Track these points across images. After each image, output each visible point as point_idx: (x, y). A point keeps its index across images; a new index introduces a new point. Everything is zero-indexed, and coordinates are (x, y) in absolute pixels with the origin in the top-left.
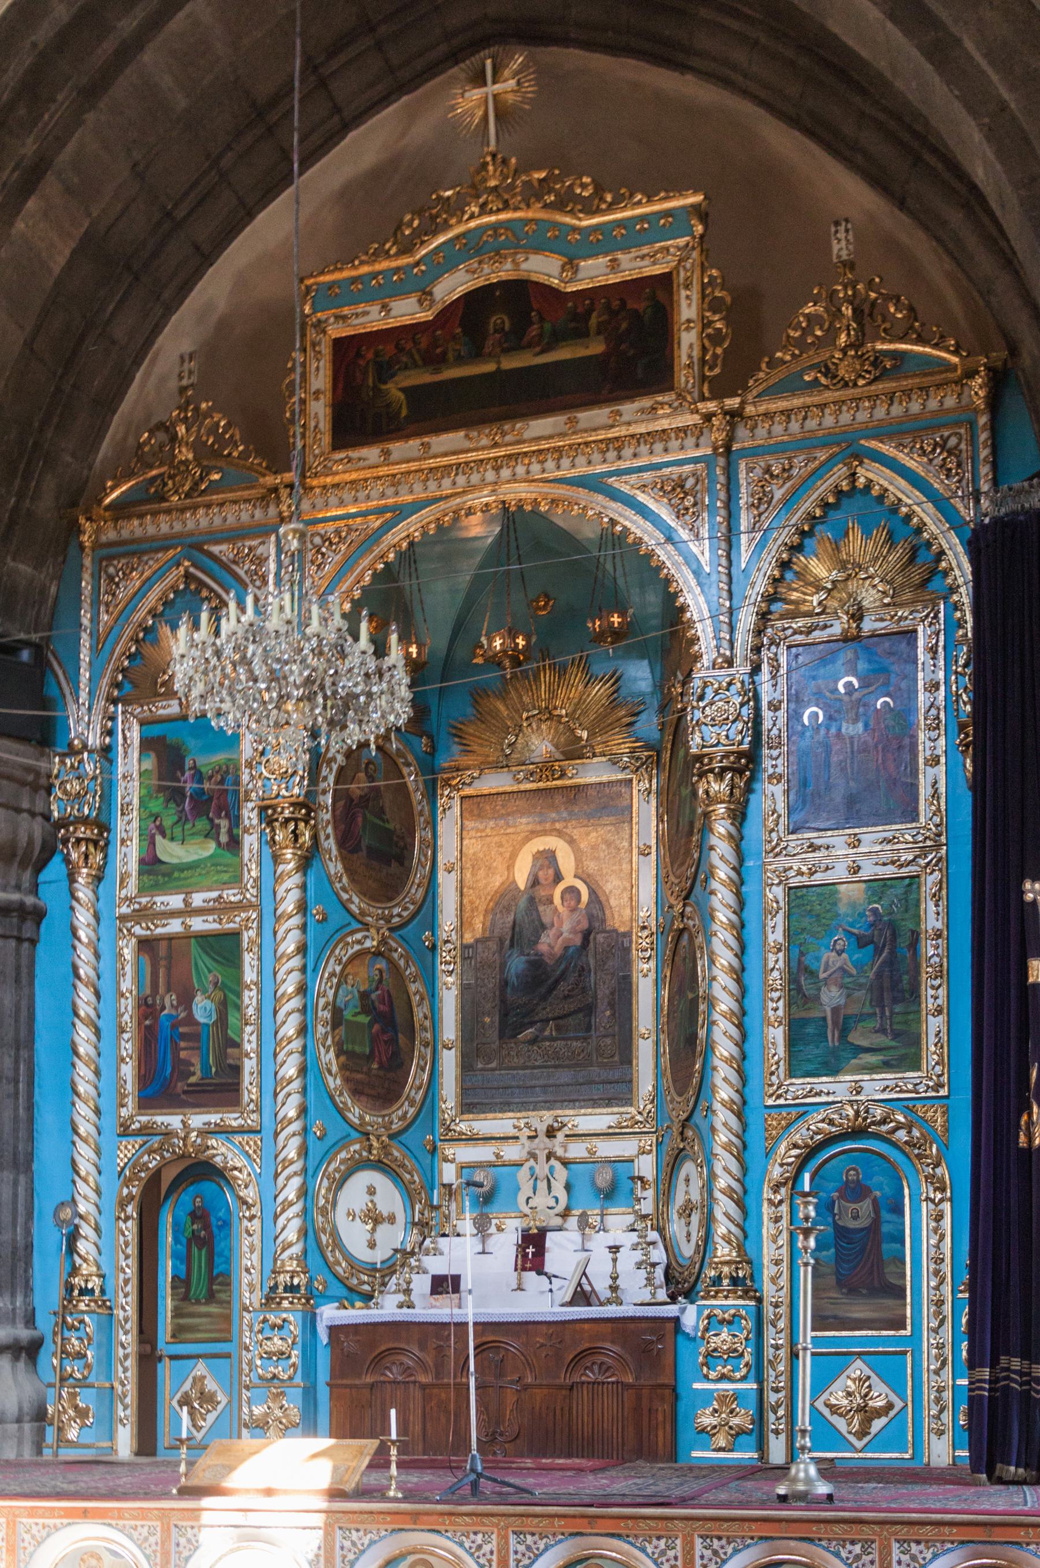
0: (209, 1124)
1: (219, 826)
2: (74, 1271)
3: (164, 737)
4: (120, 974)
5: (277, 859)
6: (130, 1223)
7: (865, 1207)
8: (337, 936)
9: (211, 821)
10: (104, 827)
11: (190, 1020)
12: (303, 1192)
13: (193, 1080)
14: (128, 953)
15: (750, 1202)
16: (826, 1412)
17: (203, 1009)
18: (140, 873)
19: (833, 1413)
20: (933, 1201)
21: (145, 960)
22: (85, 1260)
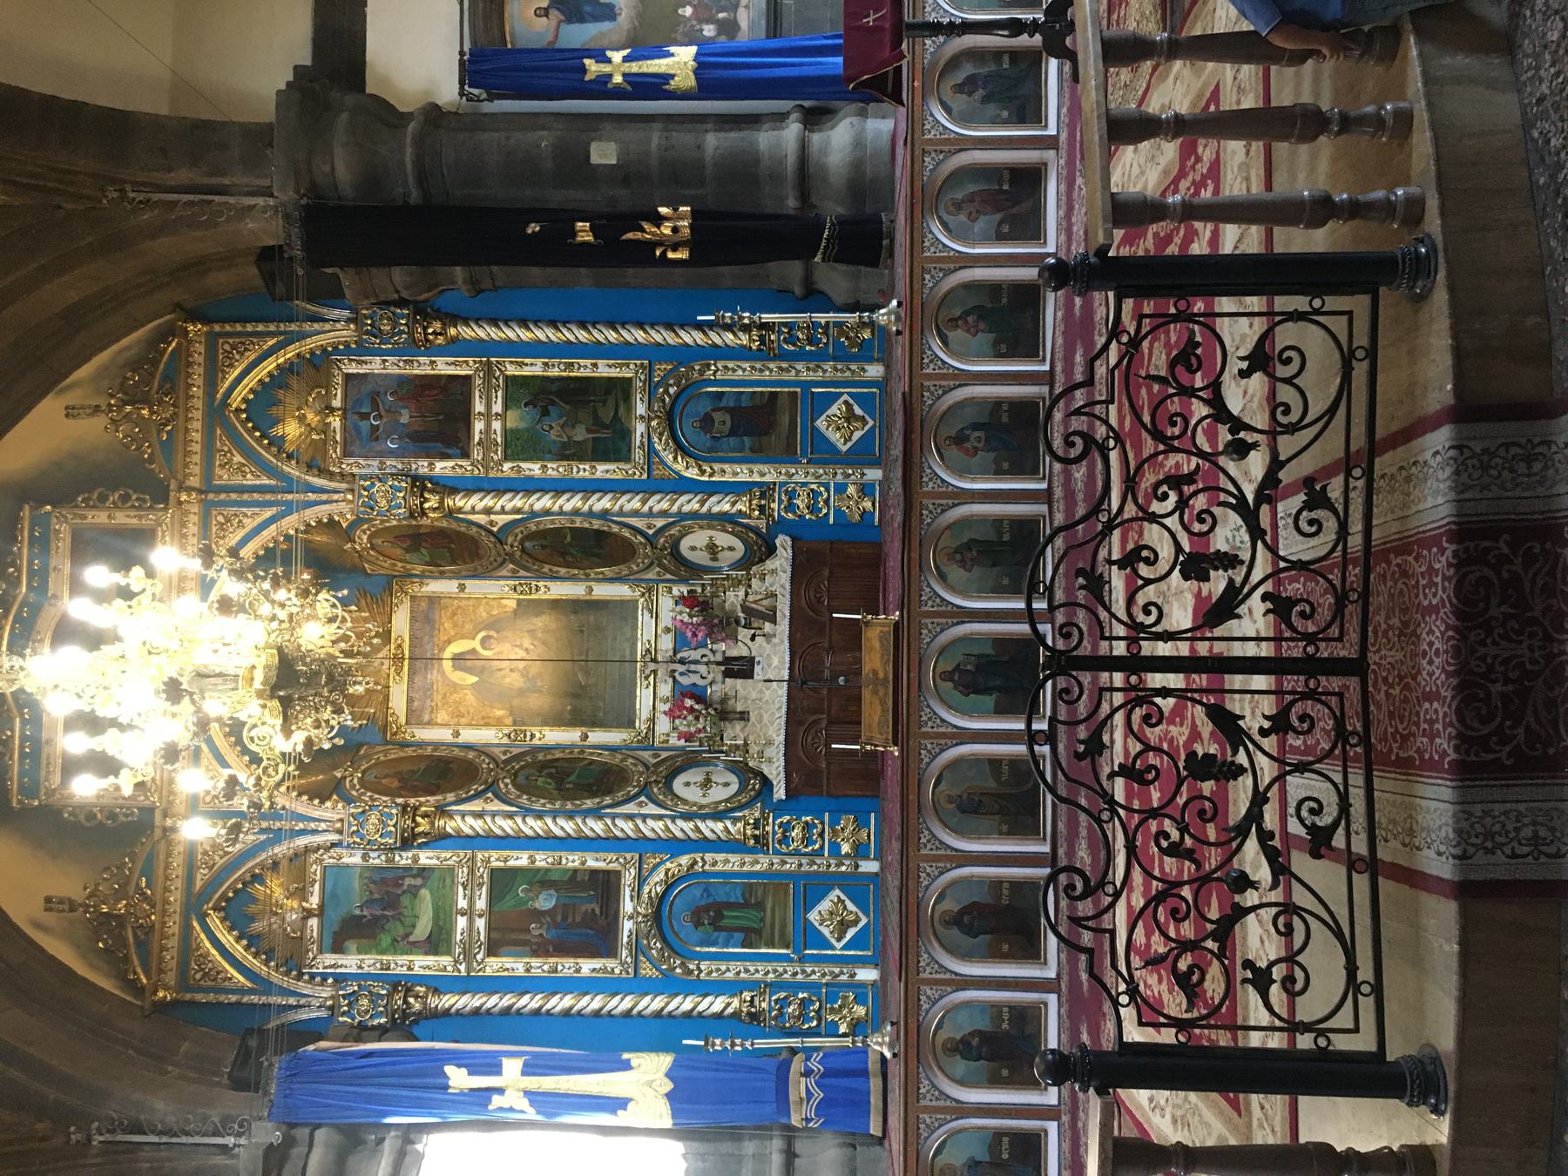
0: (632, 897)
2: (736, 1015)
3: (334, 933)
6: (702, 967)
7: (717, 416)
9: (404, 892)
12: (687, 817)
13: (598, 911)
16: (849, 444)
18: (436, 953)
19: (850, 439)
20: (715, 372)
21: (505, 949)
22: (728, 1005)
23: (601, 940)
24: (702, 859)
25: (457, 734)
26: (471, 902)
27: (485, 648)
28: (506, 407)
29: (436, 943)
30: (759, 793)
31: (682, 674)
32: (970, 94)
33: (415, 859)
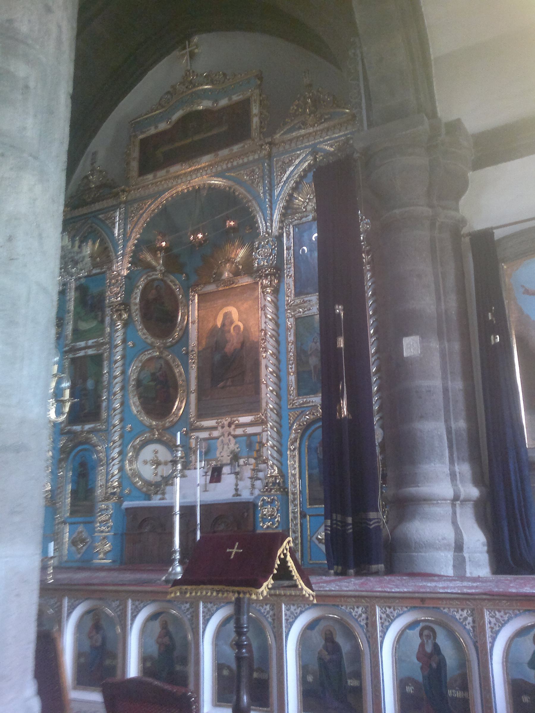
8: (141, 352)
32: (326, 648)
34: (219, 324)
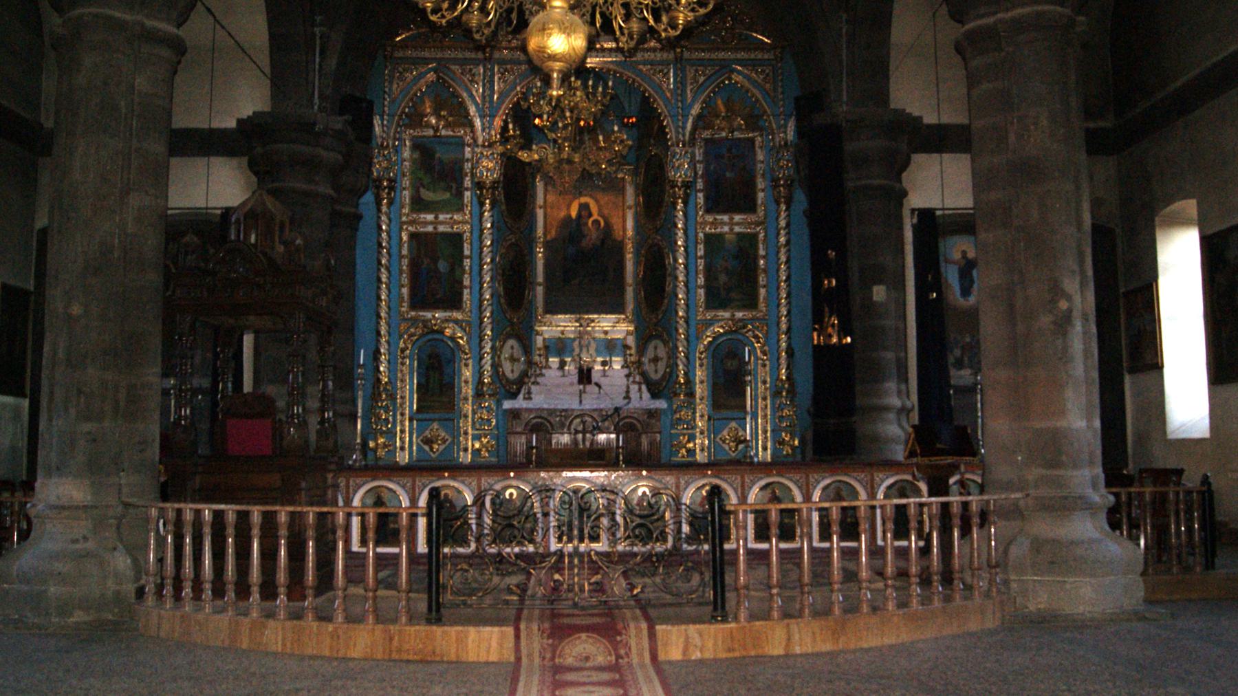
1: (452, 187)
4: (400, 246)
5: (482, 204)
7: (735, 363)
10: (395, 181)
11: (437, 271)
12: (493, 348)
13: (438, 297)
14: (405, 238)
15: (691, 357)
17: (442, 266)
23: (420, 300)
24: (469, 358)
25: (540, 208)
26: (442, 223)
27: (593, 222)
28: (738, 234)
29: (419, 204)
30: (508, 392)
31: (580, 343)
33: (467, 189)
34: (574, 214)
